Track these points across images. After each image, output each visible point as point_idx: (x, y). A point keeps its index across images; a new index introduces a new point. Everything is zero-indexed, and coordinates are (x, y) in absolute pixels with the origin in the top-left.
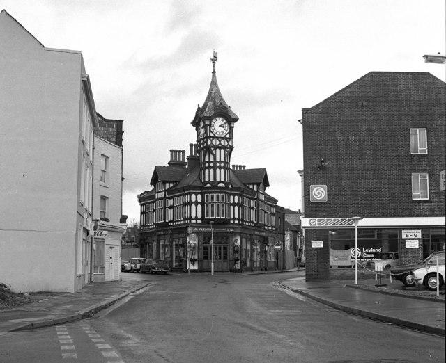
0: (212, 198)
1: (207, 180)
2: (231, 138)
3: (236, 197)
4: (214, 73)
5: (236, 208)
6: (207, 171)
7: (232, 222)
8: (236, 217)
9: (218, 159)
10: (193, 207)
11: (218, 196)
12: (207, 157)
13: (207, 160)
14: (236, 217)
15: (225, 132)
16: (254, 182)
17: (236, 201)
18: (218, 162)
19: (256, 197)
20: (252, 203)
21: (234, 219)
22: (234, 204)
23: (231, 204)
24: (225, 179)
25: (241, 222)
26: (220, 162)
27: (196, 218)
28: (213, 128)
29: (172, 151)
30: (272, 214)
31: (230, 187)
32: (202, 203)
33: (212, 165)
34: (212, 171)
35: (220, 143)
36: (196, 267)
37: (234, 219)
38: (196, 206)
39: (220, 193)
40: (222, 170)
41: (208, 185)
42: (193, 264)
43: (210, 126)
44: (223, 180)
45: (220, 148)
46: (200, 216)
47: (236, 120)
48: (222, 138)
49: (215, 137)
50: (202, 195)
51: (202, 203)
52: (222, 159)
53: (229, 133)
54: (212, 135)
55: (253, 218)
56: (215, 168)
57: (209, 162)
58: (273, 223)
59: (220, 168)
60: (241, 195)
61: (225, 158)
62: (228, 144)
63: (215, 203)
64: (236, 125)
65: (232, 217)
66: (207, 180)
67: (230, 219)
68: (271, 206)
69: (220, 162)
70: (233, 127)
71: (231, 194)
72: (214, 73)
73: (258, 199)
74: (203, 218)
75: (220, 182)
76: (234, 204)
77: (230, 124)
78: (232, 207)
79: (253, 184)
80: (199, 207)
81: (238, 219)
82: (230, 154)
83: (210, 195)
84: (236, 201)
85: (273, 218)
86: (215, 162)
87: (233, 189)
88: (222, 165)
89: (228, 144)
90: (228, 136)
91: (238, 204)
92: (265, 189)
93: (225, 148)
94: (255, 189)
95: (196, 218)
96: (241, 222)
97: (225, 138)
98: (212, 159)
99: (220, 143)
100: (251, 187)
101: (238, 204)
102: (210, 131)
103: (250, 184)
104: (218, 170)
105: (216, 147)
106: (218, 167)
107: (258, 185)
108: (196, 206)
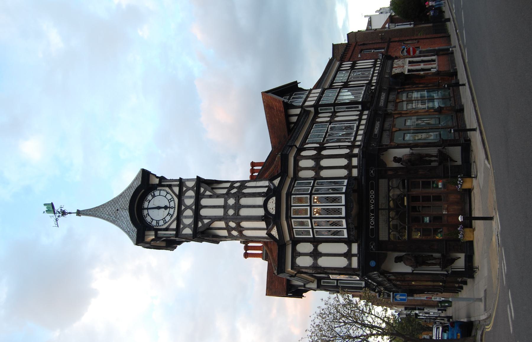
0: (302, 224)
1: (263, 233)
2: (181, 182)
3: (303, 163)
4: (79, 213)
5: (324, 163)
6: (247, 233)
7: (355, 172)
8: (344, 162)
9: (220, 212)
10: (323, 262)
11: (297, 212)
12: (225, 233)
13: (225, 233)
14: (344, 162)
15: (169, 197)
16: (283, 115)
17: (311, 163)
18: (226, 212)
19: (312, 109)
20: (324, 118)
21: (348, 167)
22: (318, 168)
23: (317, 177)
24: (259, 195)
25: (356, 151)
26: (225, 207)
27: (348, 255)
28: (161, 223)
29: (246, 255)
30: (353, 67)
31: (276, 182)
32: (316, 242)
33: (232, 224)
34: (244, 224)
35: (189, 207)
36: (462, 256)
37: (348, 167)
38: (321, 255)
39: (289, 207)
40: (244, 201)
41: (274, 232)
42: (454, 260)
43: (156, 230)
44: (260, 201)
45: (198, 207)
46: (343, 248)
47: (145, 174)
48: (180, 203)
49: (179, 219)
50: (295, 242)
51: (316, 242)
52: (220, 202)
53: (170, 186)
54: (174, 226)
55: (352, 115)
56: (238, 218)
57: (228, 229)
58: (368, 63)
59: (238, 207)
60: (302, 149)
61: (219, 196)
62: (192, 189)
63: (311, 218)
64: (157, 170)
65: (344, 172)
66: (263, 233)
67: (349, 177)
68: (338, 70)
69: (225, 207)
70: (162, 179)
71: (296, 177)
72: (79, 213)
73: (317, 106)
74: (348, 242)
75: (265, 206)
76: (318, 168)
77: (154, 188)
78: (324, 173)
79: (288, 116)
80: (323, 248)
81: (348, 157)
82: (211, 184)
83: (296, 228)
84: (311, 163)
85: (362, 64)
86: (225, 218)
87: (283, 174)
88: (231, 201)
89: (192, 189)
90: (176, 190)
91: (317, 158)
92: (301, 89)
93: (198, 197)
94: (298, 111)
95: (348, 255)
96: (356, 151)
97: (180, 196)
98: (222, 224)
99: (189, 207)
100: (294, 119)
101: (317, 158)
102: (167, 229)
103: (288, 123)
104: (244, 212)
105: (197, 217)
106: (237, 213)
107: (288, 106)
108: (321, 255)
